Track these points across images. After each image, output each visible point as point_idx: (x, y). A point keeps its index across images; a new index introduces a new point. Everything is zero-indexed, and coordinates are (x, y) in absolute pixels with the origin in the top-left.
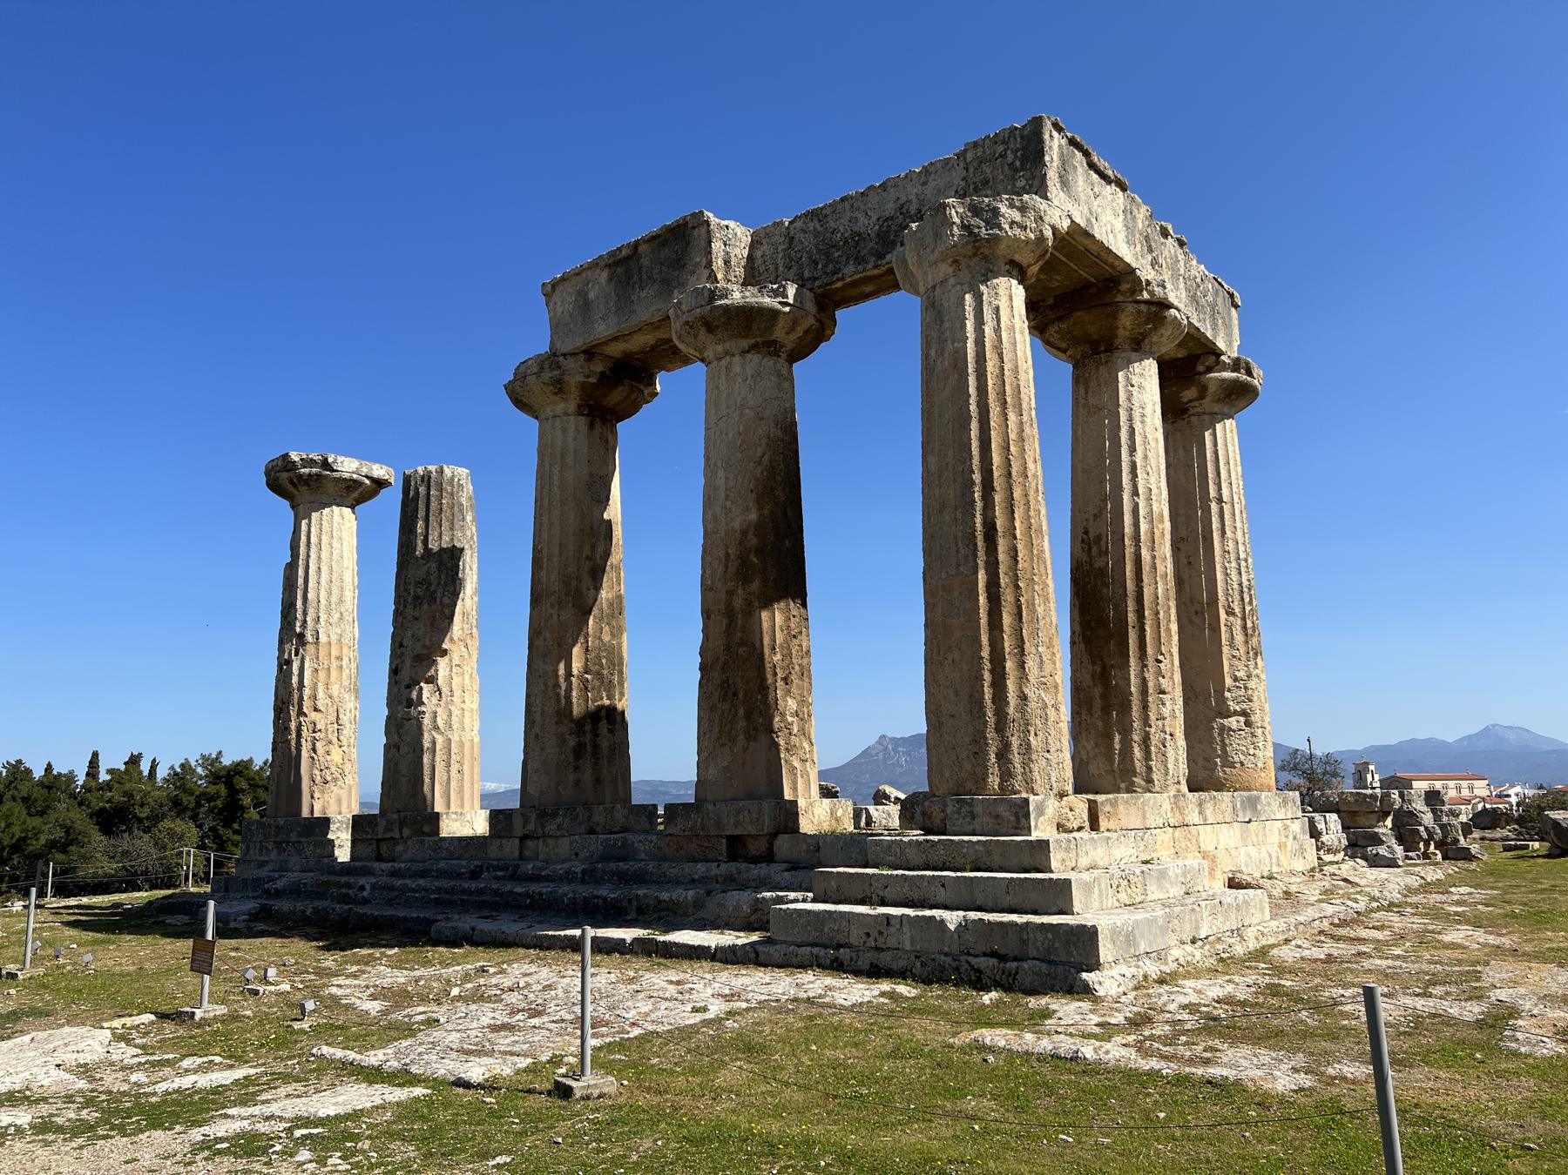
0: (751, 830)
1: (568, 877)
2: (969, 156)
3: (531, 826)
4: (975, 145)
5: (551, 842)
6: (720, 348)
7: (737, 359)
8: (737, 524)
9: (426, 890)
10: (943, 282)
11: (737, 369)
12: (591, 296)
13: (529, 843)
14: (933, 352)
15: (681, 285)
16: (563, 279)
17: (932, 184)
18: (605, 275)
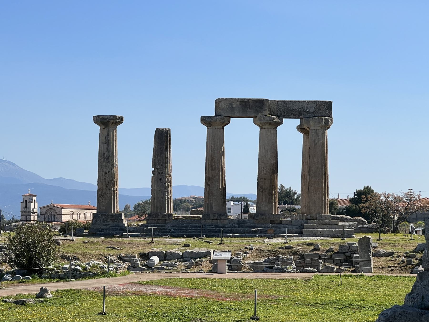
0: (277, 219)
1: (234, 227)
2: (317, 103)
3: (216, 217)
4: (319, 101)
5: (222, 221)
6: (269, 127)
7: (272, 130)
8: (272, 162)
9: (195, 230)
10: (319, 130)
11: (272, 132)
12: (234, 106)
13: (214, 221)
14: (316, 141)
15: (262, 112)
16: (226, 99)
17: (309, 106)
18: (238, 103)
